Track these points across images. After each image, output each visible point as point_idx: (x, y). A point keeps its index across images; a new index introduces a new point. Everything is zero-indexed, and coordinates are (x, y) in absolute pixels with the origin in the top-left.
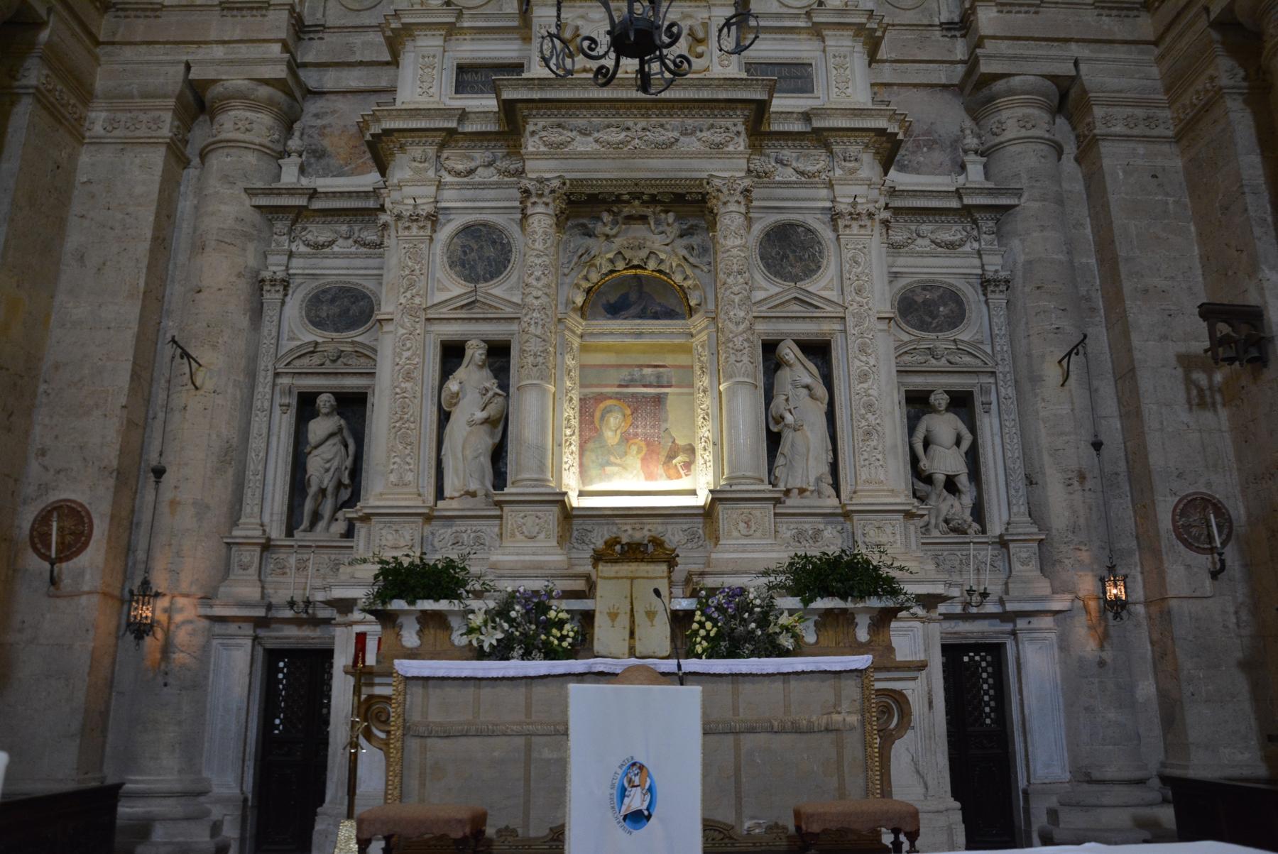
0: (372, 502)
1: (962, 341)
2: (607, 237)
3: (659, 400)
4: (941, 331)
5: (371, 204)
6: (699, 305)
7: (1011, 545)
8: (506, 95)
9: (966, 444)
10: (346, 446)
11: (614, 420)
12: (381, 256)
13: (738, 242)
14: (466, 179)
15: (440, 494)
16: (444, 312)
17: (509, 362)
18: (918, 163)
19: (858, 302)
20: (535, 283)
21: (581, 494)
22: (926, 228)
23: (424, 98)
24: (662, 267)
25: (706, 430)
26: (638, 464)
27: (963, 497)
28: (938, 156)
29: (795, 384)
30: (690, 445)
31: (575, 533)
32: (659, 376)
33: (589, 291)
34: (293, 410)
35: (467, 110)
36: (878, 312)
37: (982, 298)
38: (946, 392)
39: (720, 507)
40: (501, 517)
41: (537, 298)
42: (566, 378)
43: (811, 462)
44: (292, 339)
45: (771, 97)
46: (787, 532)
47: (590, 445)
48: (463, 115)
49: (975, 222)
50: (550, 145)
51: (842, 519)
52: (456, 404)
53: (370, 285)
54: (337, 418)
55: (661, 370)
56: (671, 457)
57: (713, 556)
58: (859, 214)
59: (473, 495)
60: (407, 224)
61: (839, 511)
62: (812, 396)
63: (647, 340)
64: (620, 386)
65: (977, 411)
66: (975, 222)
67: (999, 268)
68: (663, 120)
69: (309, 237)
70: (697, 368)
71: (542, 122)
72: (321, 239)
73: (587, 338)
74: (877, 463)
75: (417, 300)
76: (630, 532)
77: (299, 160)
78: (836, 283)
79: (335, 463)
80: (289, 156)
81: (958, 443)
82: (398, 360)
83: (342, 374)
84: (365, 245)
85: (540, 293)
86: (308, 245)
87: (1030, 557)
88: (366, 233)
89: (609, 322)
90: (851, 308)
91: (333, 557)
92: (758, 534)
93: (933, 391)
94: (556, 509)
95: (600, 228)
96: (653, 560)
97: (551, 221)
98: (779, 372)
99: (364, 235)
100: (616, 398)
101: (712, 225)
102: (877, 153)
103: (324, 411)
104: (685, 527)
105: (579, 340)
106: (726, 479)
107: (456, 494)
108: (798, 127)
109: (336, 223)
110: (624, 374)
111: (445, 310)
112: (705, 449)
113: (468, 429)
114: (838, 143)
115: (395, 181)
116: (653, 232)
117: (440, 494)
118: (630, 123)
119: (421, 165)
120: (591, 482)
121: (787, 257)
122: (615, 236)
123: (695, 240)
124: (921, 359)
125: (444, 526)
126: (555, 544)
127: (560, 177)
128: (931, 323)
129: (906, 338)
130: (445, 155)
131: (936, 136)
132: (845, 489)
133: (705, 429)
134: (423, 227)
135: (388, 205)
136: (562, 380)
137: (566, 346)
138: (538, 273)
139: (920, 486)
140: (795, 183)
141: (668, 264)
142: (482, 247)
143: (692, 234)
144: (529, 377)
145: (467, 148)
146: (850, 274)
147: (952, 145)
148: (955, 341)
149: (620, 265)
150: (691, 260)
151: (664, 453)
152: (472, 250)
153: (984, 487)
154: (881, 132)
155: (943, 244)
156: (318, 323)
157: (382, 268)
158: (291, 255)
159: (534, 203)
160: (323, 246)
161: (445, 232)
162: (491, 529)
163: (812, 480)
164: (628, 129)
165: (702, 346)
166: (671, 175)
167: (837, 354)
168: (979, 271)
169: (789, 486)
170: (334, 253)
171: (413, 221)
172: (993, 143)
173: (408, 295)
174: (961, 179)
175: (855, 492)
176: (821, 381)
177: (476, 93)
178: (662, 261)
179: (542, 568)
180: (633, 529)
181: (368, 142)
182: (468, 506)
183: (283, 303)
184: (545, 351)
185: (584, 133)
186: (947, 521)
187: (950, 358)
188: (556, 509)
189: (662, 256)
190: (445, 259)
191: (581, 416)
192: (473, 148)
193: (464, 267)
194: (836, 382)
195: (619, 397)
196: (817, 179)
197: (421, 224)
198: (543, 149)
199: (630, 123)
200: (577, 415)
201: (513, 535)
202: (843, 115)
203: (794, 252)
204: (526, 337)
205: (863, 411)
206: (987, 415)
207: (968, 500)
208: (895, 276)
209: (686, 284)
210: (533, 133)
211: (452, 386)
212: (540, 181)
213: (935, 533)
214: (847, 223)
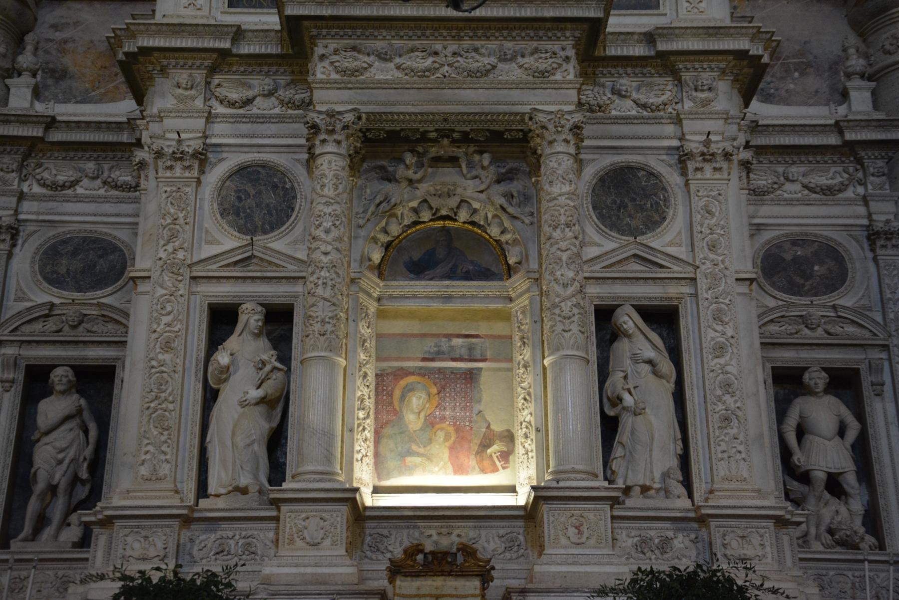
0: (116, 501)
1: (844, 307)
2: (411, 182)
3: (471, 377)
4: (816, 295)
5: (125, 137)
6: (520, 263)
8: (289, 11)
9: (852, 434)
10: (86, 432)
11: (417, 400)
12: (137, 201)
13: (566, 188)
14: (241, 111)
15: (202, 490)
16: (214, 269)
17: (291, 330)
18: (787, 91)
19: (713, 261)
20: (323, 236)
21: (376, 490)
22: (795, 170)
23: (190, 12)
24: (476, 218)
25: (527, 414)
26: (446, 454)
27: (851, 501)
28: (813, 82)
29: (635, 359)
30: (509, 431)
31: (368, 539)
32: (471, 349)
33: (388, 246)
34: (18, 388)
35: (243, 27)
36: (737, 272)
37: (870, 255)
38: (824, 369)
39: (545, 508)
40: (277, 519)
41: (326, 254)
42: (359, 350)
43: (657, 454)
44: (18, 299)
45: (607, 15)
46: (627, 541)
47: (388, 431)
48: (238, 33)
49: (859, 161)
50: (343, 72)
51: (695, 525)
52: (226, 380)
53: (122, 234)
54: (76, 396)
55: (474, 340)
56: (485, 445)
57: (537, 568)
58: (713, 155)
59: (244, 491)
60: (169, 163)
61: (692, 515)
62: (656, 373)
63: (456, 305)
64: (424, 359)
66: (859, 161)
67: (891, 217)
68: (478, 43)
69: (46, 175)
70: (516, 338)
71: (333, 45)
72: (61, 178)
73: (384, 302)
74: (738, 456)
75: (180, 255)
76: (435, 537)
77: (33, 81)
78: (685, 236)
79: (71, 453)
80: (20, 75)
81: (842, 431)
82: (155, 326)
83: (84, 342)
84: (116, 187)
85: (329, 248)
86: (44, 185)
88: (117, 173)
89: (412, 283)
90: (703, 267)
91: (60, 573)
92: (592, 541)
93: (808, 368)
94: (345, 509)
95: (401, 171)
96: (463, 574)
97: (343, 163)
98: (616, 344)
99: (115, 174)
100: (419, 374)
101: (536, 168)
102: (735, 80)
103: (59, 388)
104: (502, 532)
105: (375, 304)
106: (554, 473)
107: (223, 491)
108: (639, 50)
109: (80, 159)
110: (429, 345)
111: (214, 267)
112: (526, 436)
113: (240, 410)
114: (688, 70)
115: (155, 111)
116: (464, 176)
117: (202, 490)
118: (438, 47)
119: (187, 93)
120: (388, 477)
121: (626, 207)
122: (420, 181)
123: (515, 187)
124: (791, 328)
125: (205, 531)
126: (343, 552)
127: (354, 110)
128: (803, 285)
129: (772, 303)
130: (216, 82)
131: (811, 58)
132: (699, 487)
133: (526, 412)
134: (189, 168)
135: (145, 139)
136: (355, 352)
137: (361, 310)
138: (327, 224)
139: (794, 485)
140: (636, 118)
141: (482, 214)
142: (260, 192)
143: (512, 179)
144: (315, 347)
145: (243, 73)
146: (702, 226)
147: (830, 68)
148: (834, 307)
149: (426, 216)
150: (510, 210)
151: (476, 441)
152: (248, 195)
153: (879, 490)
154: (741, 55)
155: (818, 189)
156: (54, 280)
157: (137, 216)
158: (21, 196)
159: (324, 141)
160: (63, 187)
161: (215, 175)
162: (264, 534)
163: (657, 475)
164: (436, 53)
165: (523, 312)
166: (487, 109)
167: (686, 323)
168: (865, 222)
169: (629, 483)
170: (76, 196)
171: (176, 159)
172: (885, 63)
173: (170, 248)
174: (842, 110)
175: (711, 492)
176: (667, 355)
177: (254, 7)
178: (475, 211)
179: (325, 583)
180: (439, 534)
181: (120, 62)
182: (237, 506)
183: (10, 255)
184: (335, 317)
185: (384, 57)
186: (831, 532)
187: (829, 327)
188: (345, 509)
189: (476, 205)
190: (215, 206)
191: (377, 395)
192: (251, 73)
193: (238, 215)
194: (685, 356)
195: (423, 373)
196: (662, 113)
197: (187, 164)
198: (334, 76)
199: (438, 47)
200: (372, 394)
201: (292, 541)
202: (694, 35)
203: (634, 200)
204: (311, 300)
205: (719, 392)
206: (877, 399)
207: (857, 505)
208: (757, 229)
209: (504, 238)
210: (323, 57)
211: (222, 358)
212: (331, 114)
213: (817, 546)
214: (698, 165)
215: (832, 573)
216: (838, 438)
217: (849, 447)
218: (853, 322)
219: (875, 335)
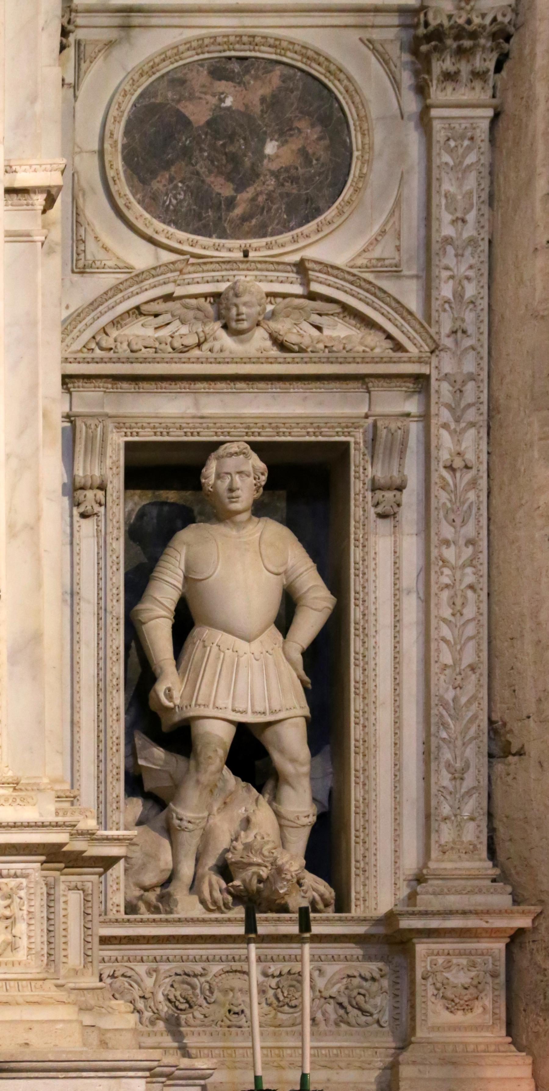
4: (261, 232)
7: (421, 948)
27: (287, 793)
38: (256, 447)
65: (355, 512)
87: (478, 986)
93: (216, 445)
128: (231, 203)
206: (385, 526)
215: (215, 968)
216: (274, 631)
217: (298, 658)
218: (348, 311)
219: (398, 347)
